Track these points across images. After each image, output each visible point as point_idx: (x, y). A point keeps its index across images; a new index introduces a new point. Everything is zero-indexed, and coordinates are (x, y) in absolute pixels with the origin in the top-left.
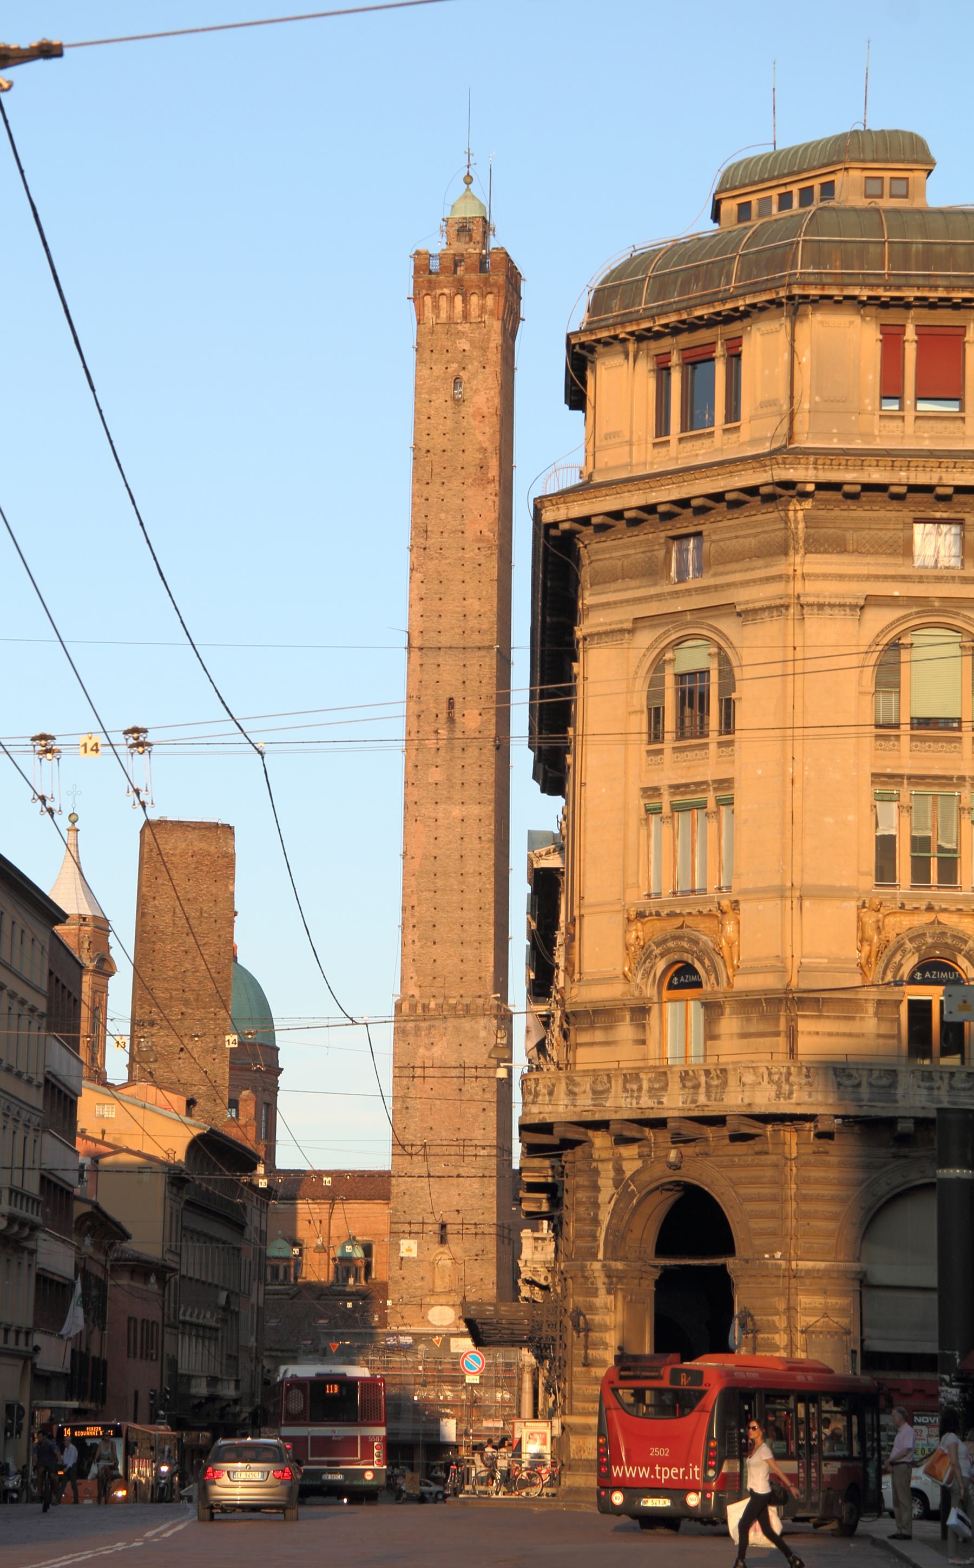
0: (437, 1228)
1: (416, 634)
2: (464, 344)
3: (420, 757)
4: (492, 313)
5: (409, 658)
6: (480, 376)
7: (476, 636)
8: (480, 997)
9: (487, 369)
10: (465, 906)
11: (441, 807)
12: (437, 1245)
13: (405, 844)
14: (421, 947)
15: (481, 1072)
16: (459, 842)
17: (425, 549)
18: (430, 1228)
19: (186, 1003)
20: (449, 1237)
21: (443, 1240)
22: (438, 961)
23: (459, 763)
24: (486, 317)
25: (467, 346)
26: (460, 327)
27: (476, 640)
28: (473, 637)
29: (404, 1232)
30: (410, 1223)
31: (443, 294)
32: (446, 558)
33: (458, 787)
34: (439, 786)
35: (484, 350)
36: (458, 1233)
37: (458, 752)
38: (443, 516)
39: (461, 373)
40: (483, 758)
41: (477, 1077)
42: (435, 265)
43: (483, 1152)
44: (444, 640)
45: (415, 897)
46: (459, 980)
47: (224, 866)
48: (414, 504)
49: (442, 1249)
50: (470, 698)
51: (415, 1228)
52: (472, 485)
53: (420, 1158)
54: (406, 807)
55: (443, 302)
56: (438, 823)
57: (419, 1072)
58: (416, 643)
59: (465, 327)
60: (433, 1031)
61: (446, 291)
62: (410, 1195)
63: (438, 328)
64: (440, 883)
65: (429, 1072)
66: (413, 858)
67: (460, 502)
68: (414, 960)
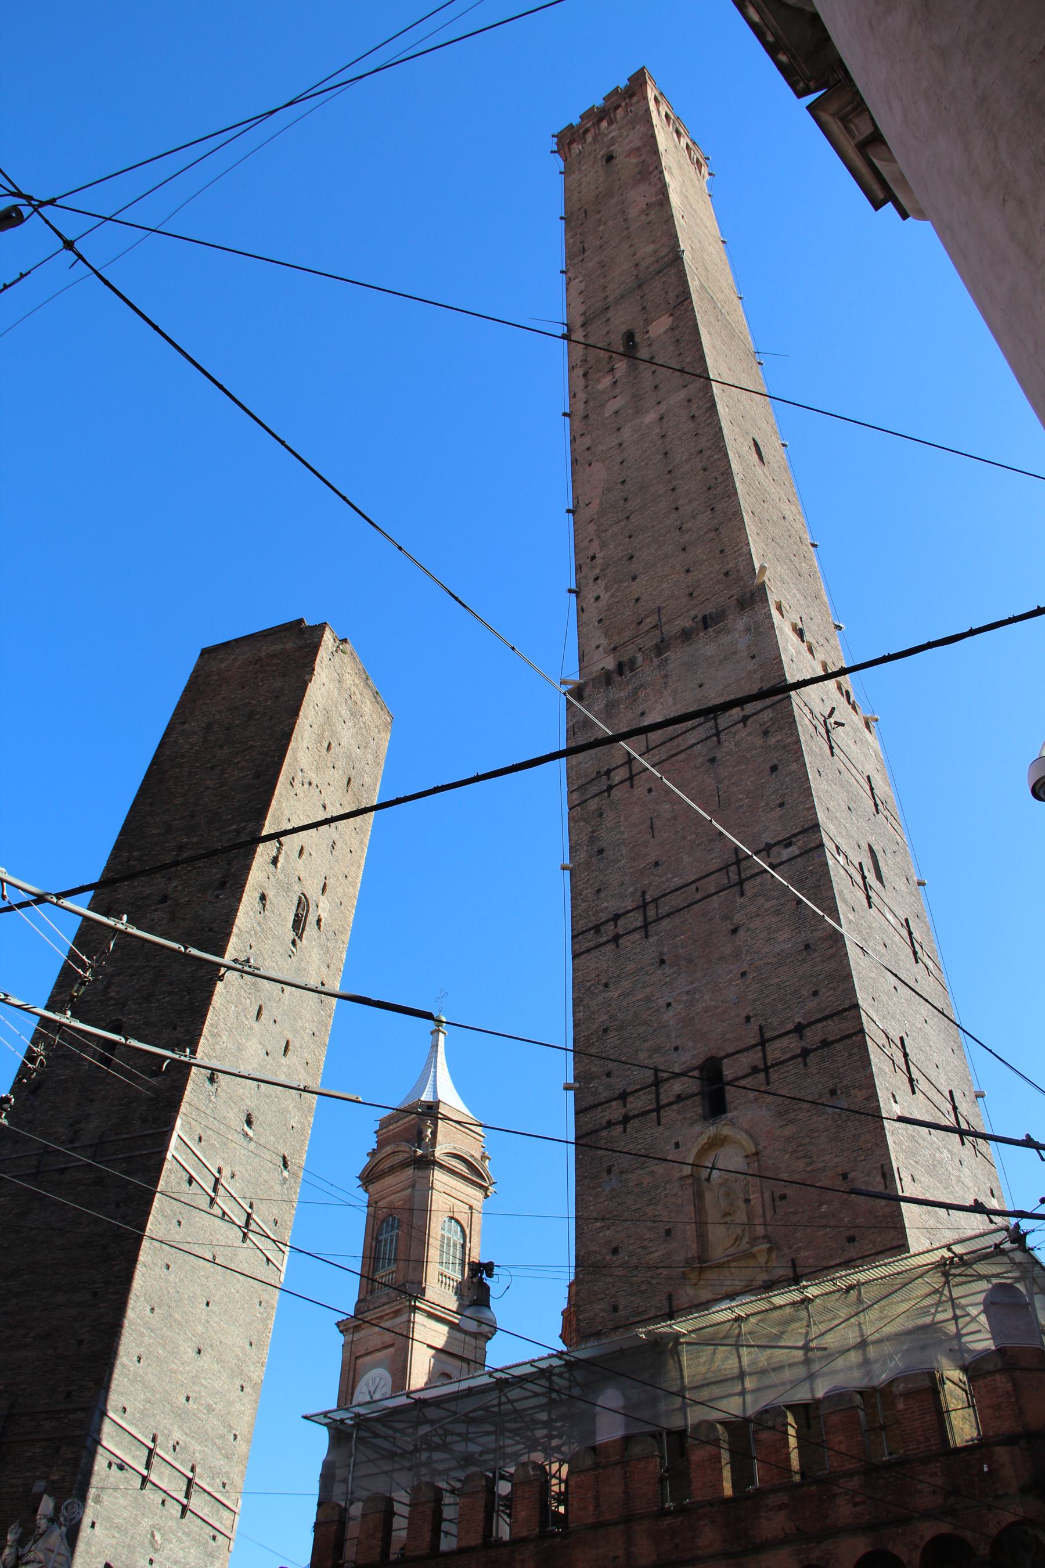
14: (612, 596)
20: (730, 1092)
21: (716, 1105)
29: (610, 1124)
30: (623, 1096)
36: (755, 1070)
38: (601, 228)
45: (596, 542)
46: (685, 600)
51: (638, 1103)
53: (636, 936)
57: (619, 775)
62: (621, 1028)
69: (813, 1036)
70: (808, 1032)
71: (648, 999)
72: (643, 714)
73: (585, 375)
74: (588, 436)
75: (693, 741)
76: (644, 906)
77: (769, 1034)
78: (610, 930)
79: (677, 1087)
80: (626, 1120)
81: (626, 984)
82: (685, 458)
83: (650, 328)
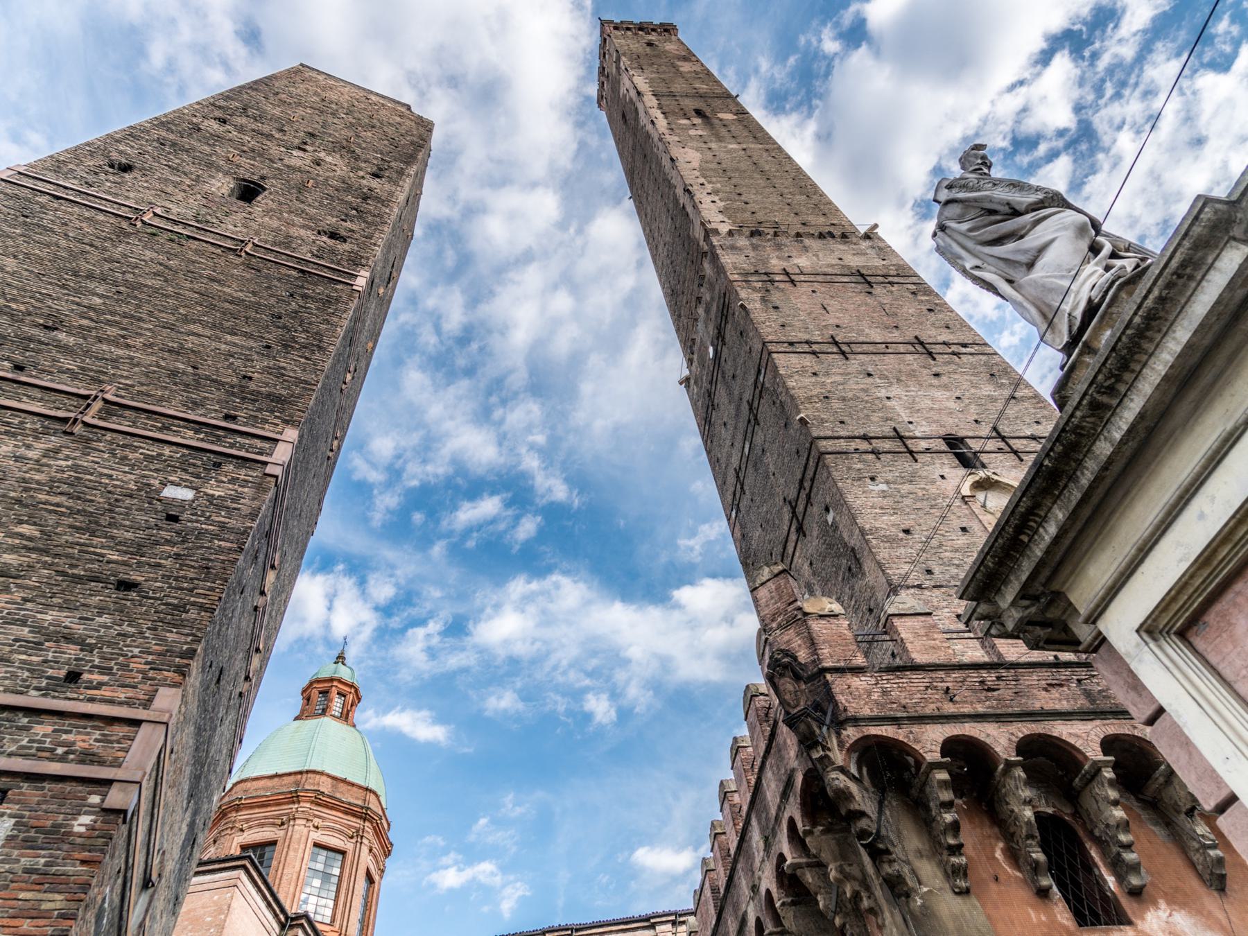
81: (838, 378)
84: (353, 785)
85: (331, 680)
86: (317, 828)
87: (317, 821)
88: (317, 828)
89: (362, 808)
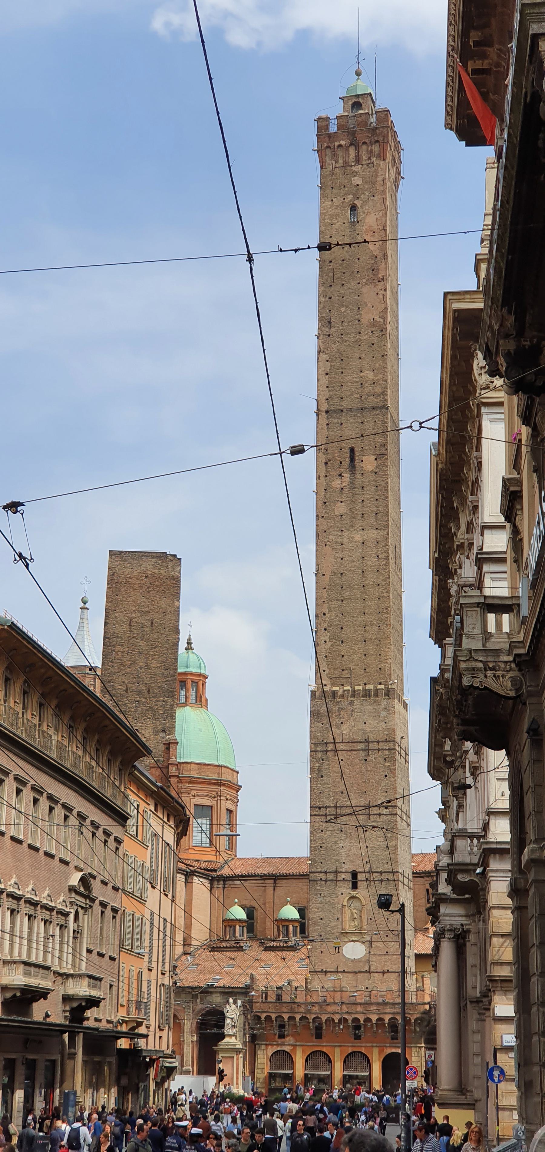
0: (349, 877)
1: (323, 400)
2: (357, 180)
3: (328, 496)
4: (379, 156)
5: (318, 419)
6: (371, 203)
7: (371, 399)
8: (380, 684)
9: (376, 198)
10: (367, 611)
11: (346, 534)
12: (349, 891)
13: (317, 565)
14: (332, 645)
15: (382, 746)
16: (361, 560)
17: (329, 335)
18: (343, 876)
19: (140, 693)
20: (359, 883)
21: (355, 886)
22: (345, 657)
23: (360, 498)
24: (374, 159)
25: (360, 182)
26: (354, 168)
27: (372, 401)
28: (369, 400)
30: (326, 873)
31: (340, 146)
32: (346, 341)
33: (359, 517)
34: (343, 517)
35: (374, 183)
37: (358, 490)
38: (343, 309)
39: (356, 202)
40: (379, 493)
41: (379, 750)
42: (333, 128)
43: (385, 811)
44: (346, 404)
46: (363, 672)
47: (172, 587)
48: (320, 303)
49: (354, 893)
50: (367, 447)
51: (331, 877)
52: (366, 284)
54: (317, 535)
55: (340, 153)
56: (344, 546)
58: (324, 407)
59: (357, 168)
60: (342, 713)
61: (342, 143)
63: (337, 170)
64: (346, 594)
65: (340, 747)
66: (324, 575)
67: (356, 297)
68: (326, 657)
69: (384, 877)
70: (383, 875)
71: (336, 842)
72: (342, 723)
73: (326, 463)
74: (326, 521)
75: (359, 748)
76: (336, 807)
77: (373, 870)
78: (323, 812)
79: (343, 876)
80: (326, 881)
82: (371, 583)
83: (364, 458)
84: (210, 765)
85: (185, 674)
86: (194, 796)
87: (194, 792)
88: (194, 796)
89: (218, 780)
